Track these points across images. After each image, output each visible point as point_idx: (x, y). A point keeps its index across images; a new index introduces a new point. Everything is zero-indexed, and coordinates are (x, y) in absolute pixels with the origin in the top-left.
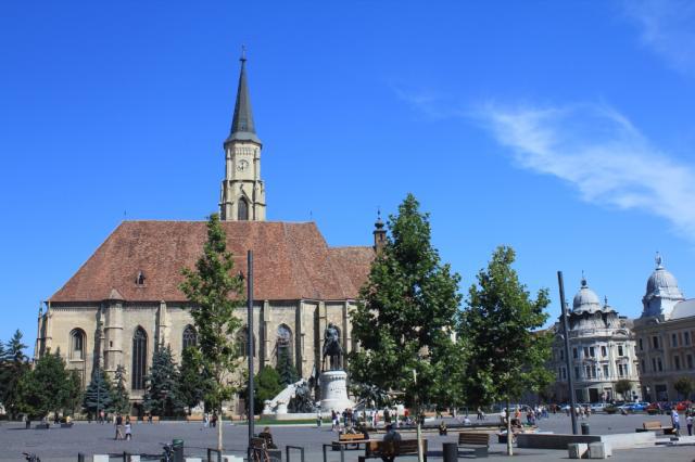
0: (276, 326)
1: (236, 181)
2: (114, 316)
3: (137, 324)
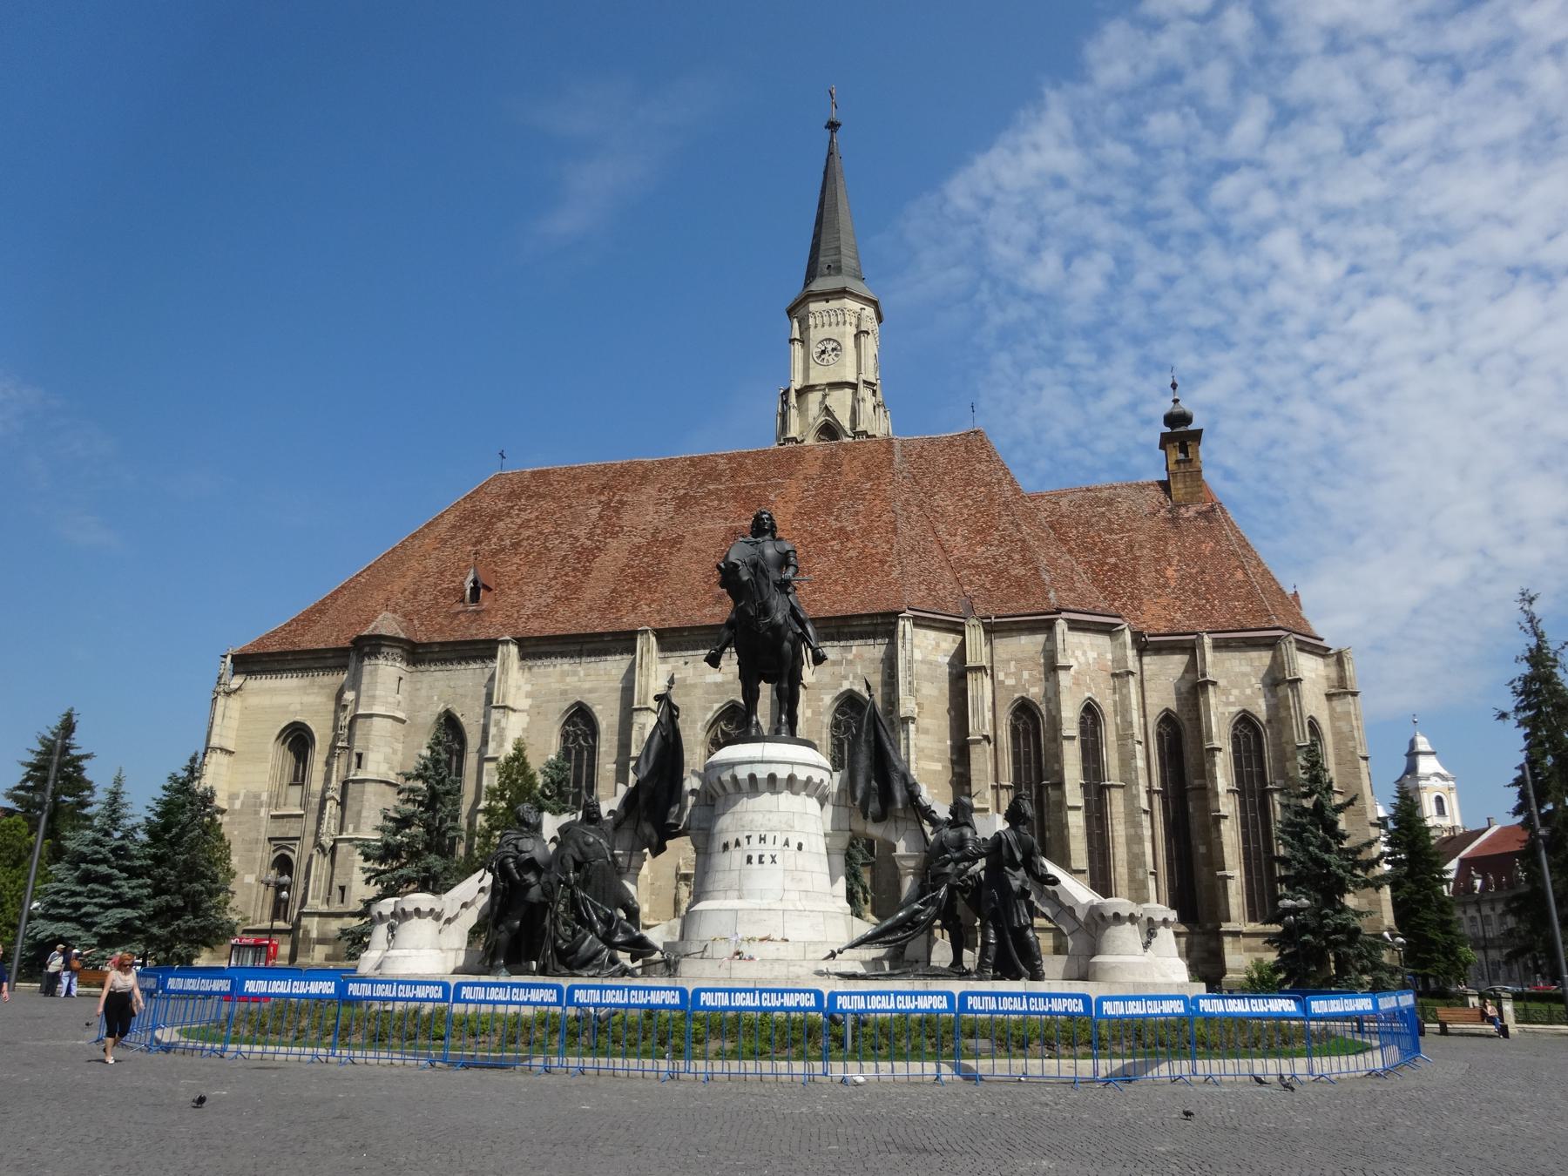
0: (828, 699)
2: (373, 684)
3: (441, 708)
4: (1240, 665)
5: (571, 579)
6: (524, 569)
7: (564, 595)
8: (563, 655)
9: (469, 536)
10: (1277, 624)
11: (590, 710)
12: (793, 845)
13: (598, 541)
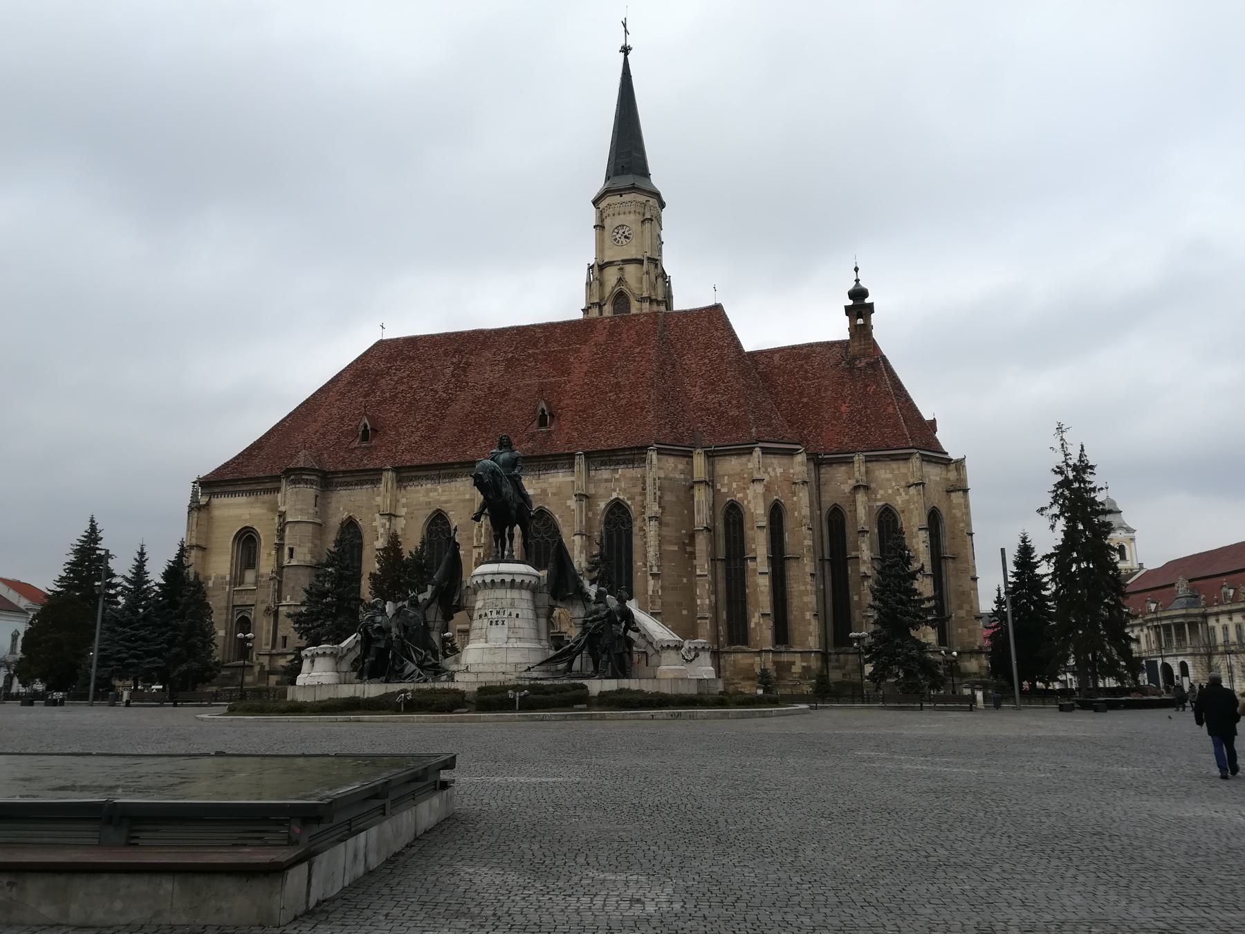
1: (610, 264)
3: (345, 515)
4: (886, 473)
5: (432, 422)
6: (400, 415)
7: (427, 434)
8: (427, 478)
9: (361, 390)
10: (911, 445)
11: (447, 515)
12: (514, 615)
13: (450, 393)
